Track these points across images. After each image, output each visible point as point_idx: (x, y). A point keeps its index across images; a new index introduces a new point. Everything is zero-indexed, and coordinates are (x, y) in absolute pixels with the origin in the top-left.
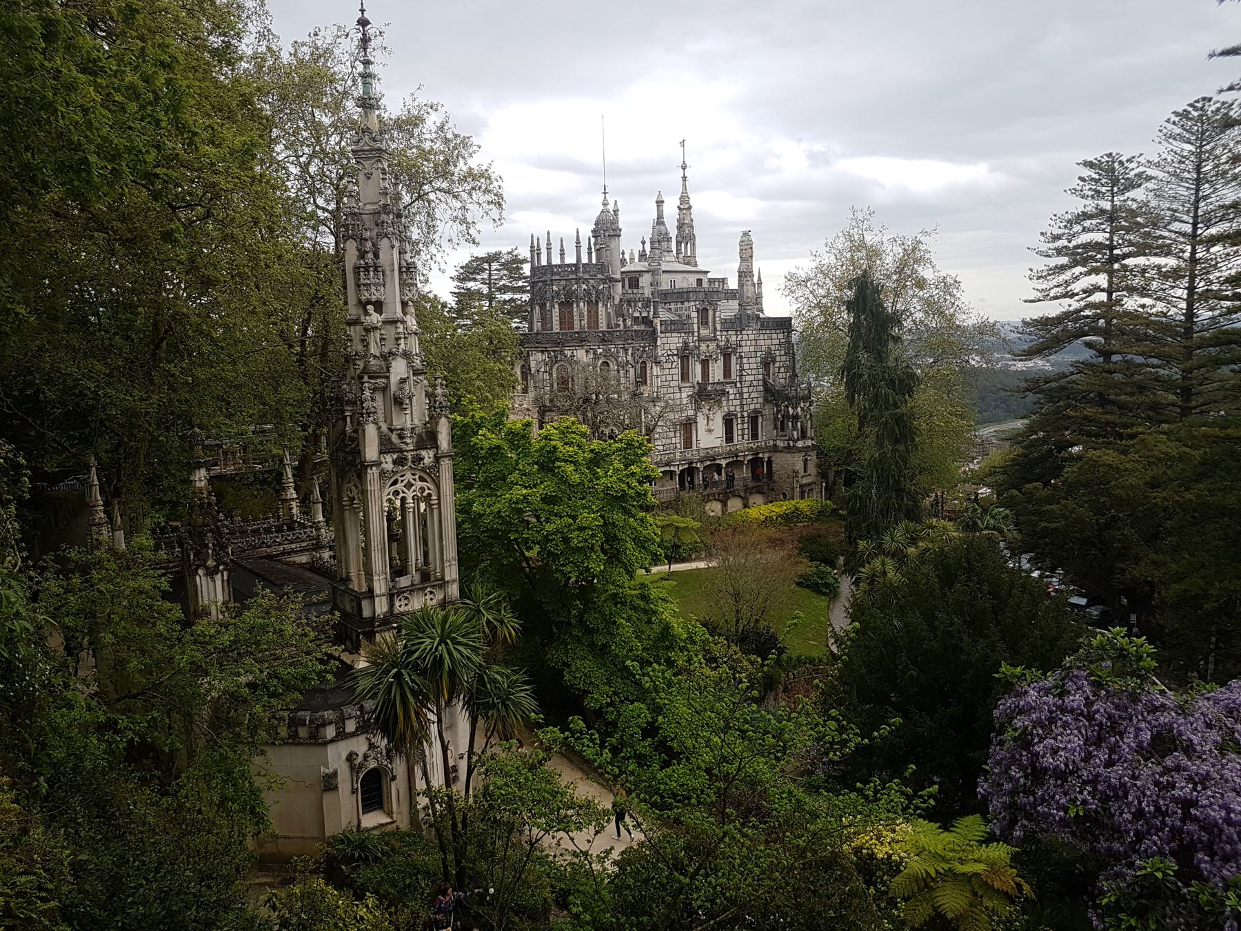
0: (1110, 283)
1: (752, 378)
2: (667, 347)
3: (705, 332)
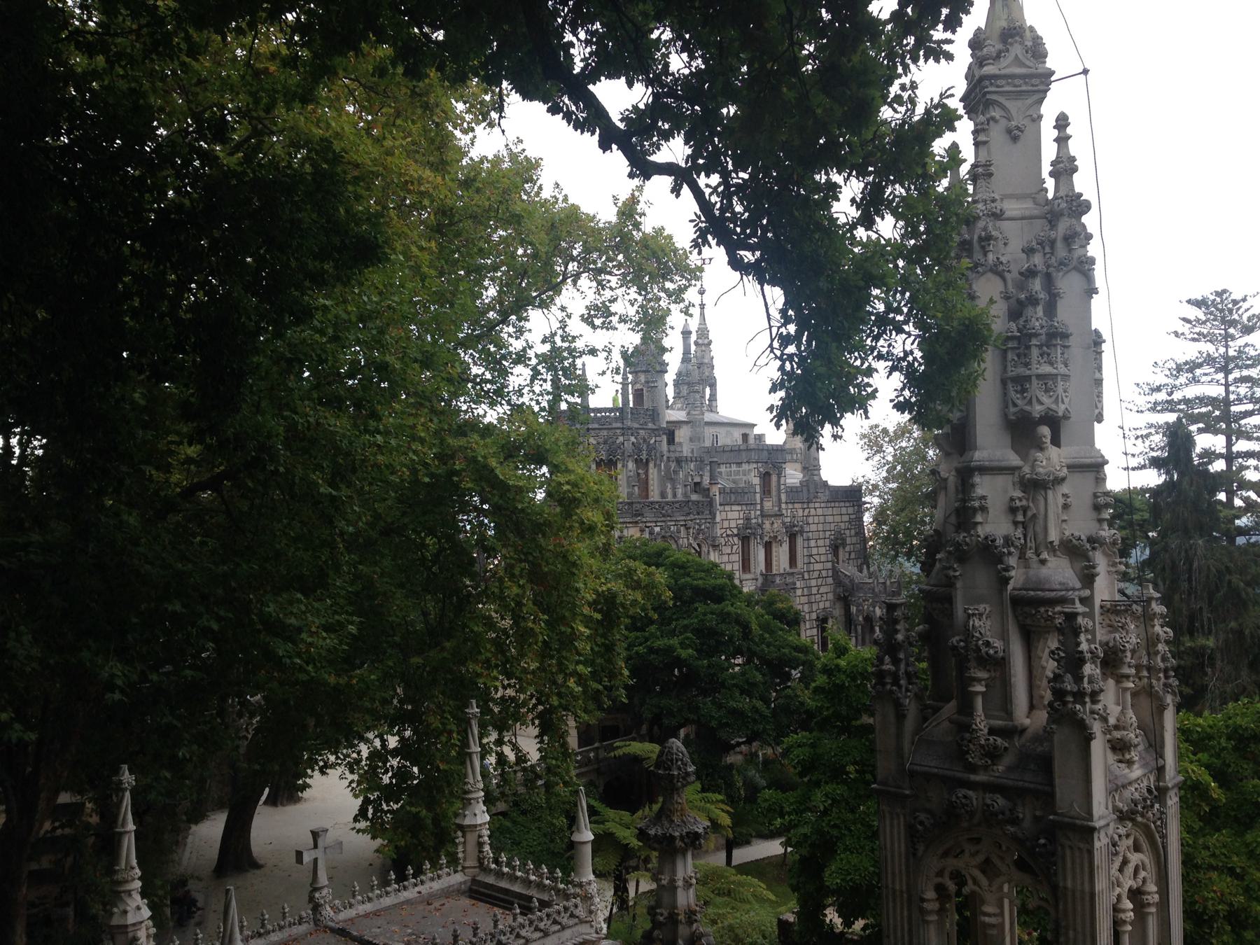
0: (1229, 444)
2: (726, 524)
3: (768, 505)
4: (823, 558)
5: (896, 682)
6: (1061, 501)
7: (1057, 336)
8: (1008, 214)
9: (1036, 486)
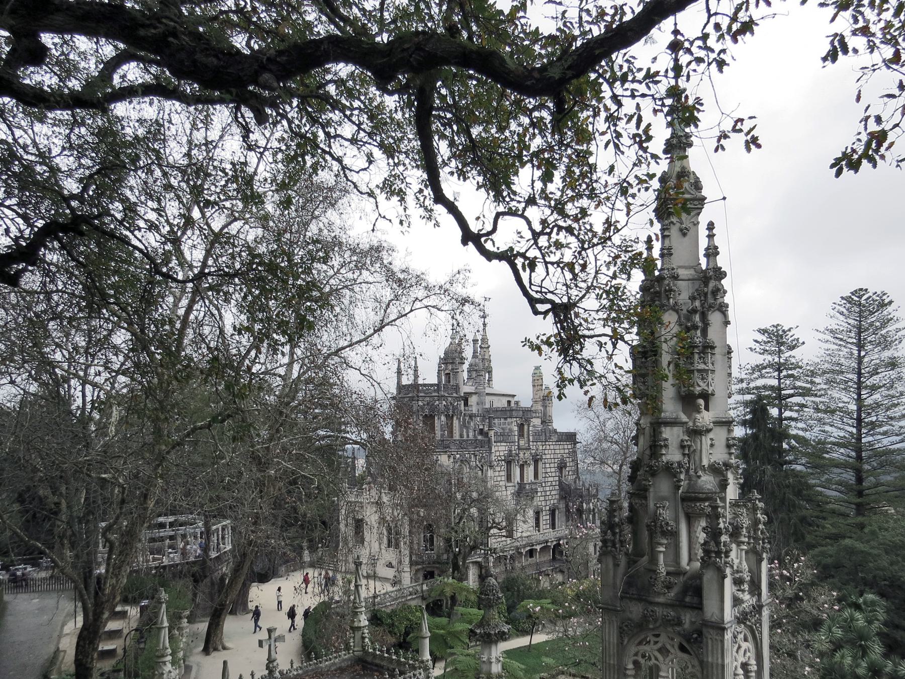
1: (551, 479)
2: (498, 454)
3: (522, 443)
4: (554, 474)
5: (614, 545)
6: (709, 442)
7: (708, 347)
8: (681, 277)
9: (696, 433)
